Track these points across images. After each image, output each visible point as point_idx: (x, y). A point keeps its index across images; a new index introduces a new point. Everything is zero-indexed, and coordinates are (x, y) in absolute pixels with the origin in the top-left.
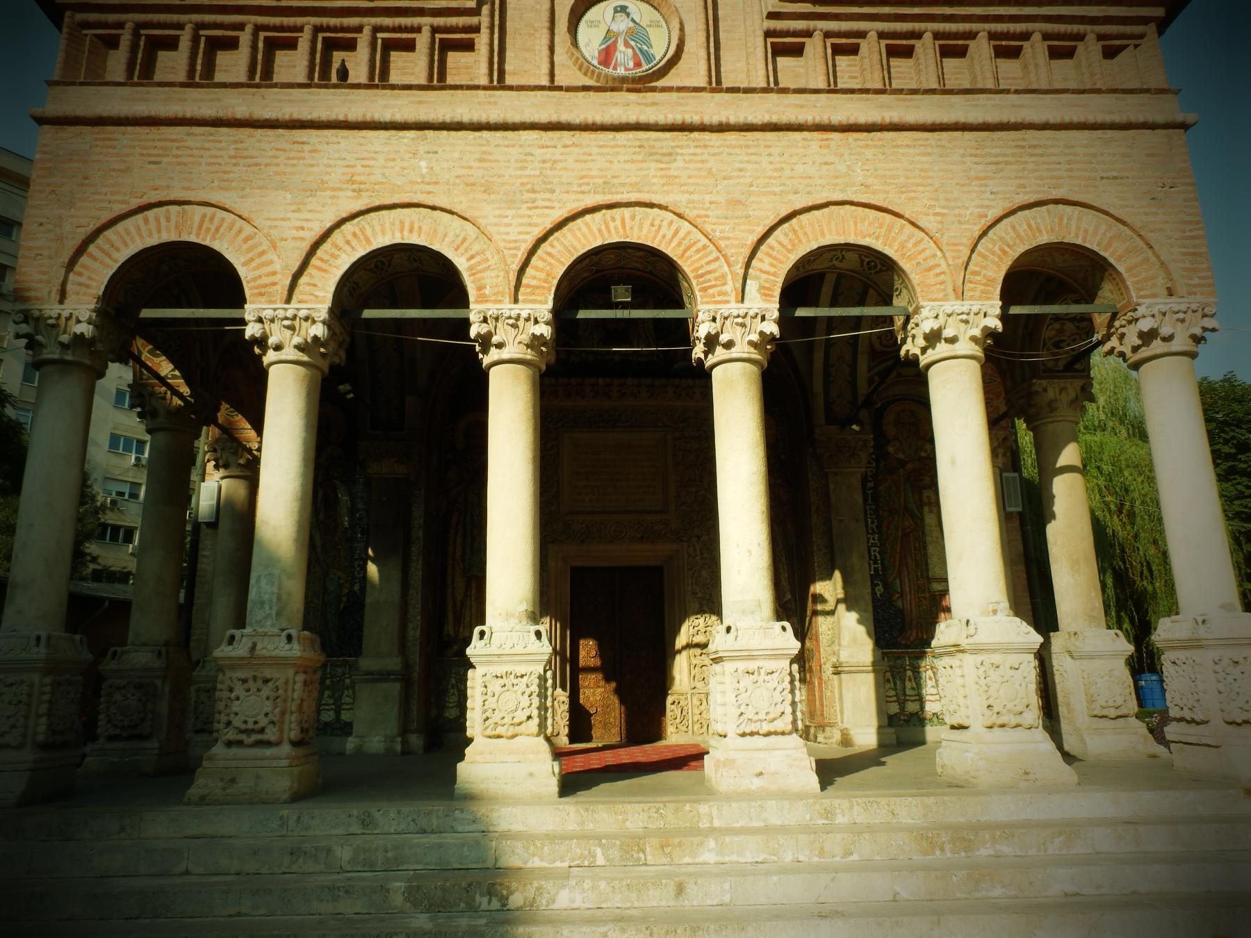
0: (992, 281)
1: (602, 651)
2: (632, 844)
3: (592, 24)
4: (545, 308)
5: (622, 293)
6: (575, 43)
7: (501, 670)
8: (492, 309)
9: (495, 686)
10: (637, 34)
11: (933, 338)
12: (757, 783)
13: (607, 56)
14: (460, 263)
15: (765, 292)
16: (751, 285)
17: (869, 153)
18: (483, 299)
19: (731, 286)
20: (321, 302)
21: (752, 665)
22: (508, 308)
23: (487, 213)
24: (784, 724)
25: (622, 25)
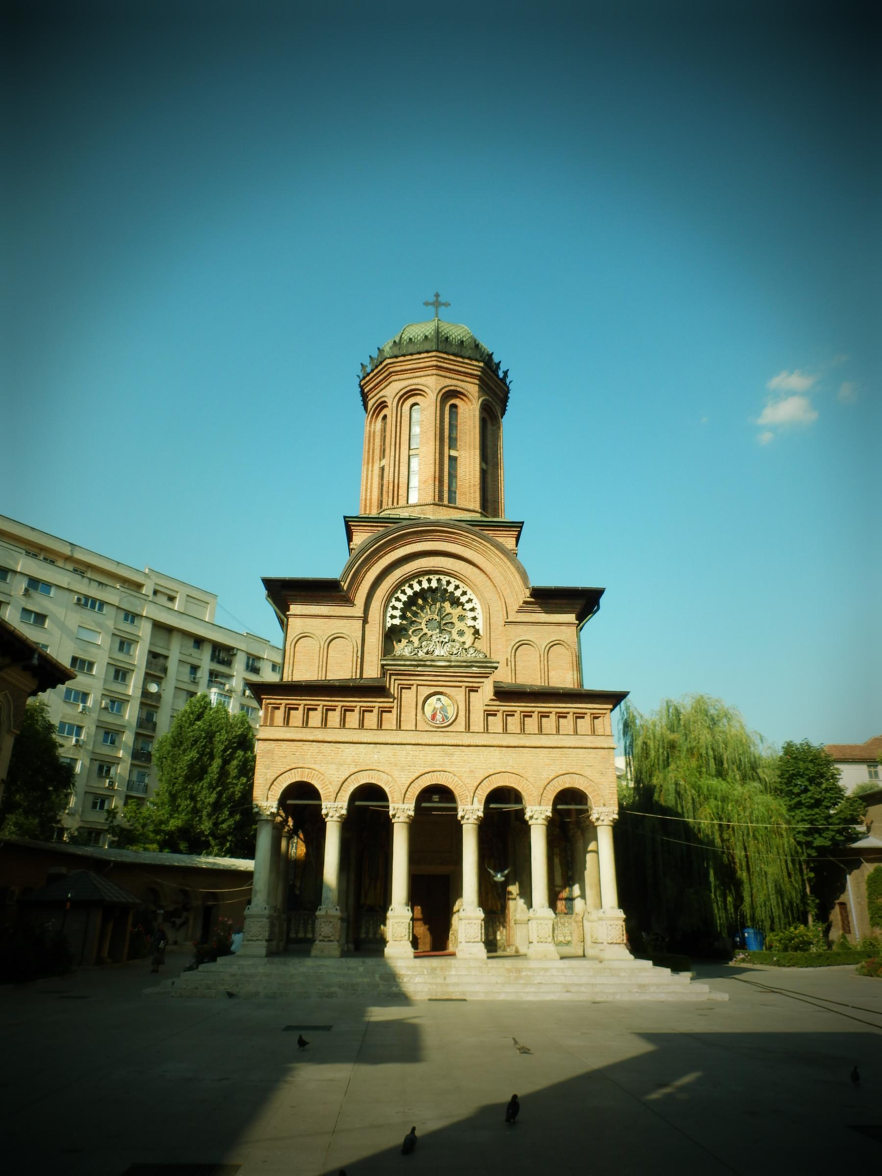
0: (549, 800)
1: (423, 912)
2: (434, 969)
3: (429, 705)
4: (412, 806)
5: (436, 798)
6: (424, 713)
7: (397, 920)
8: (396, 806)
9: (396, 926)
10: (443, 709)
11: (531, 817)
12: (469, 956)
13: (434, 717)
14: (387, 790)
15: (479, 801)
16: (476, 799)
17: (514, 755)
18: (393, 802)
19: (469, 799)
20: (344, 801)
21: (470, 921)
22: (401, 806)
23: (396, 774)
24: (479, 939)
25: (439, 705)
